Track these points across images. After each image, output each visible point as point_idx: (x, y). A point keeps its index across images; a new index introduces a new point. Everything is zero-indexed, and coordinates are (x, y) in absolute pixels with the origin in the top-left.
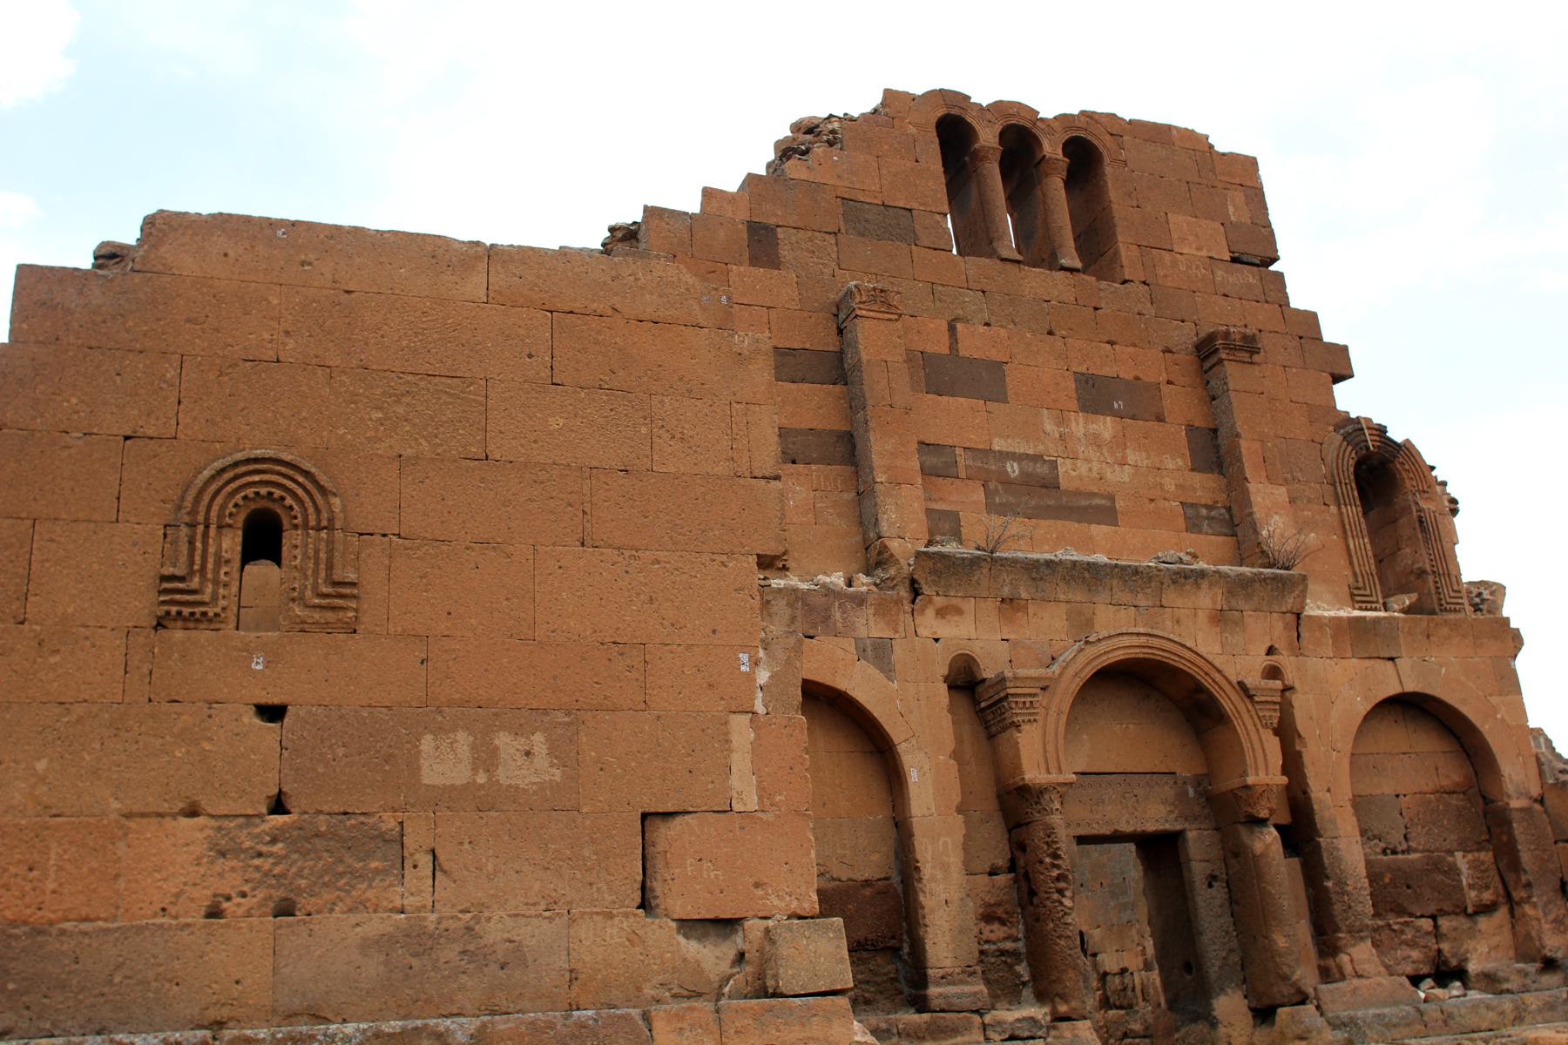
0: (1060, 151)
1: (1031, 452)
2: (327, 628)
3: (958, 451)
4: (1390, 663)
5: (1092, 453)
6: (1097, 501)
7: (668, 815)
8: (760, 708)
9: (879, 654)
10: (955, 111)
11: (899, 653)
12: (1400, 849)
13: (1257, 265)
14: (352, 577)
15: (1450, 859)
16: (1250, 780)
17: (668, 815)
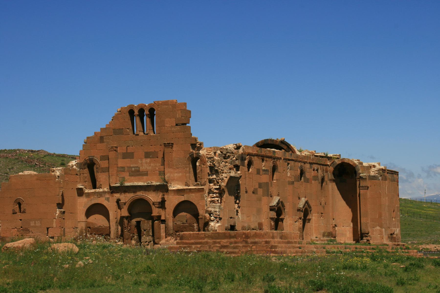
0: (148, 111)
1: (136, 166)
2: (24, 213)
3: (126, 167)
4: (183, 196)
5: (146, 165)
6: (145, 173)
7: (49, 228)
8: (56, 218)
9: (108, 199)
10: (131, 109)
11: (110, 199)
12: (185, 223)
13: (181, 125)
14: (25, 208)
15: (193, 225)
16: (152, 215)
17: (49, 228)
